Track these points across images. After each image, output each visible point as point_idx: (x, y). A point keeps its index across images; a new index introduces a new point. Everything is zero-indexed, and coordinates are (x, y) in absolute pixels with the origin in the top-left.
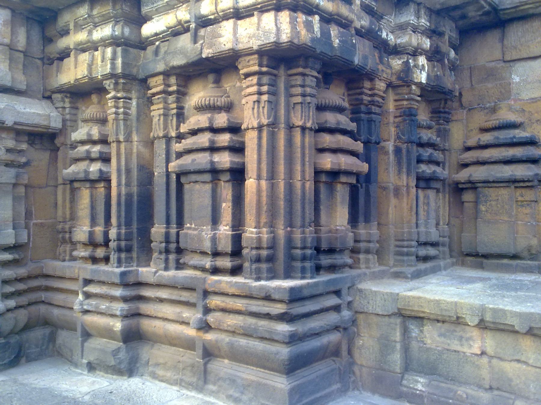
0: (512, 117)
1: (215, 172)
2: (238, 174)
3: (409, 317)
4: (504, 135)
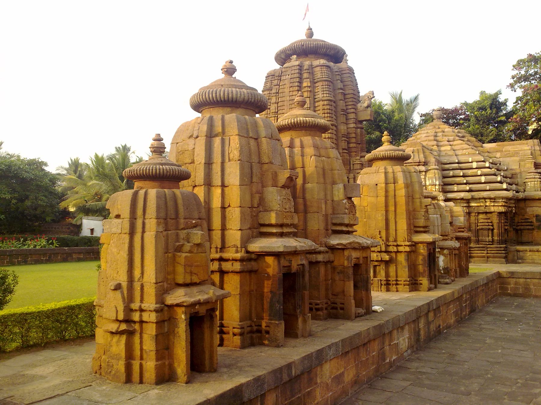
0: (527, 217)
1: (489, 229)
2: (493, 230)
3: (518, 251)
4: (526, 220)
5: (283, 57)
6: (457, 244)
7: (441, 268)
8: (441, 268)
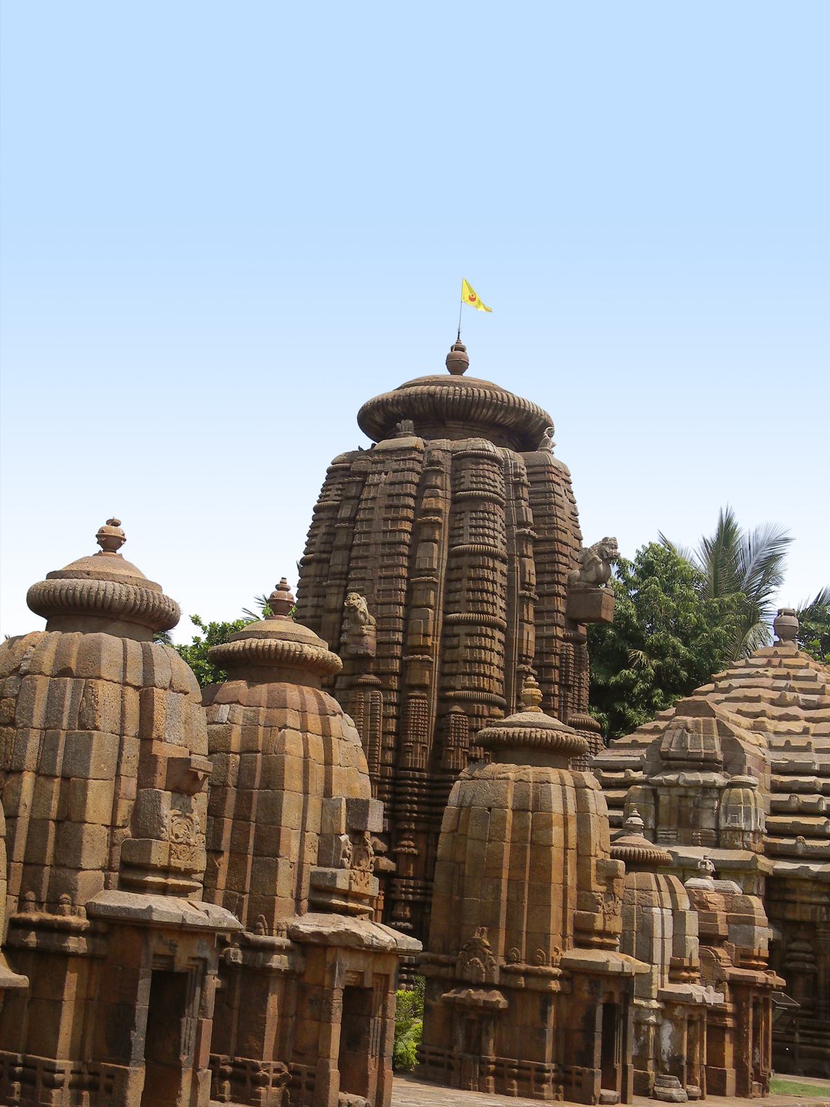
5: (377, 418)
6: (714, 997)
7: (665, 1057)
8: (665, 1057)
